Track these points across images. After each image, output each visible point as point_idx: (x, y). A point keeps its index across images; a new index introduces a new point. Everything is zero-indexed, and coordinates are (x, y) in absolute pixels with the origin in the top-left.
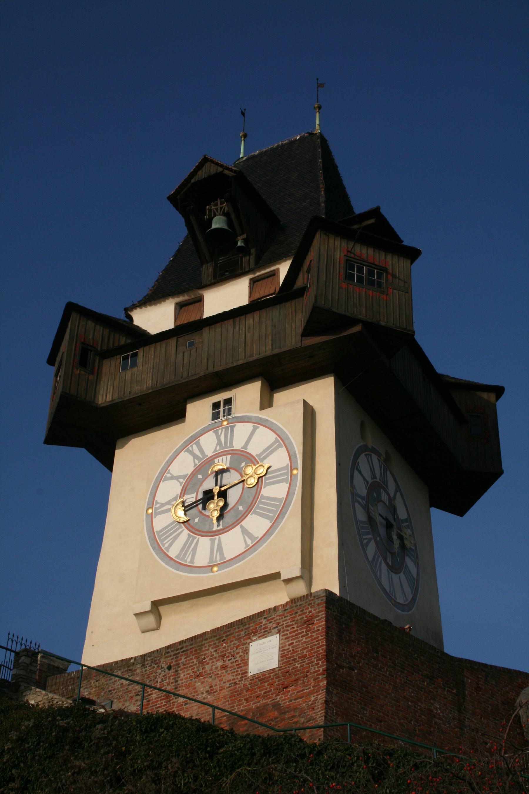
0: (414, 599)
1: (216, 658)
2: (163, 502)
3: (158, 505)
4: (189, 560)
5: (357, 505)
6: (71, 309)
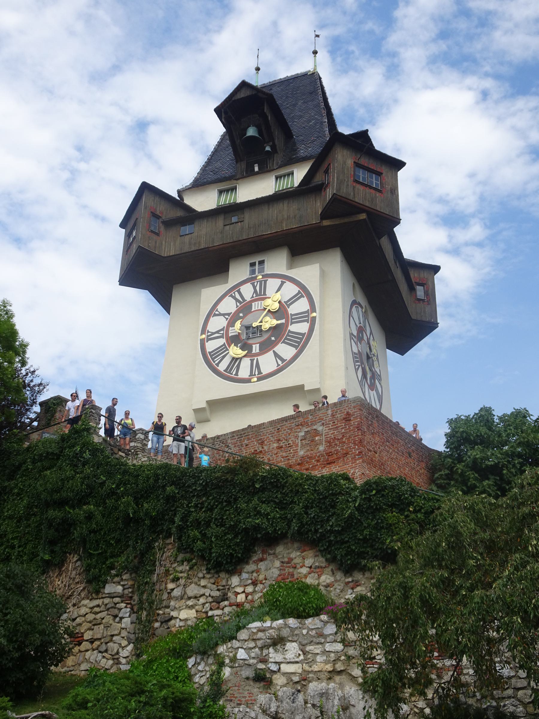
1: (272, 441)
2: (214, 331)
3: (209, 334)
4: (234, 373)
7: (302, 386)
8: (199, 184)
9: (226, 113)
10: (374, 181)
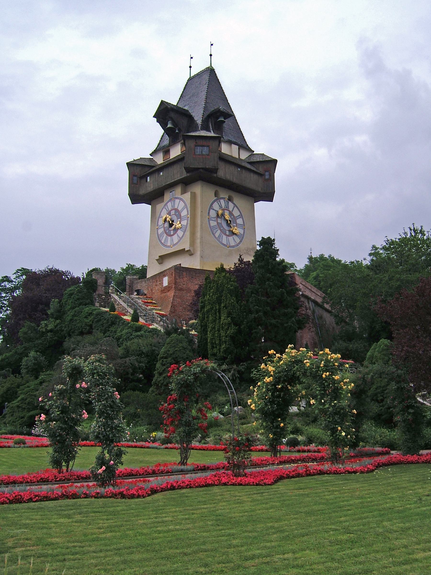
0: (241, 241)
5: (211, 222)
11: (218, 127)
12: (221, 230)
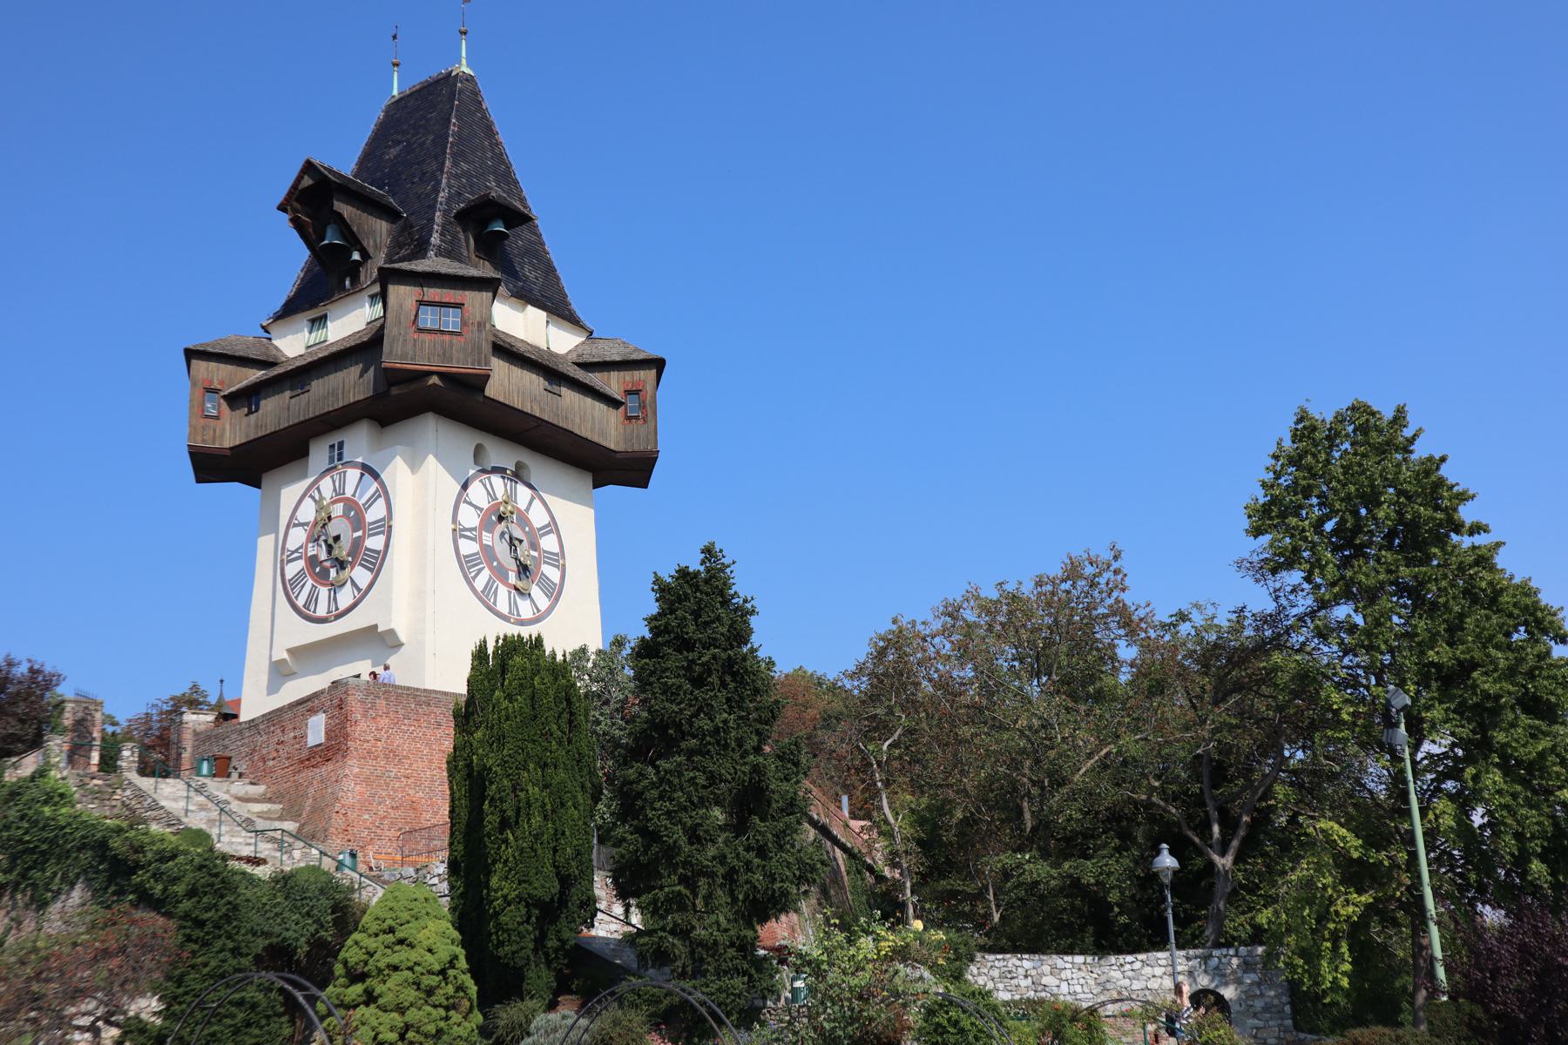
5: (462, 542)
6: (191, 354)
7: (376, 626)
8: (290, 310)
9: (294, 210)
10: (451, 320)
11: (490, 247)
12: (491, 568)
